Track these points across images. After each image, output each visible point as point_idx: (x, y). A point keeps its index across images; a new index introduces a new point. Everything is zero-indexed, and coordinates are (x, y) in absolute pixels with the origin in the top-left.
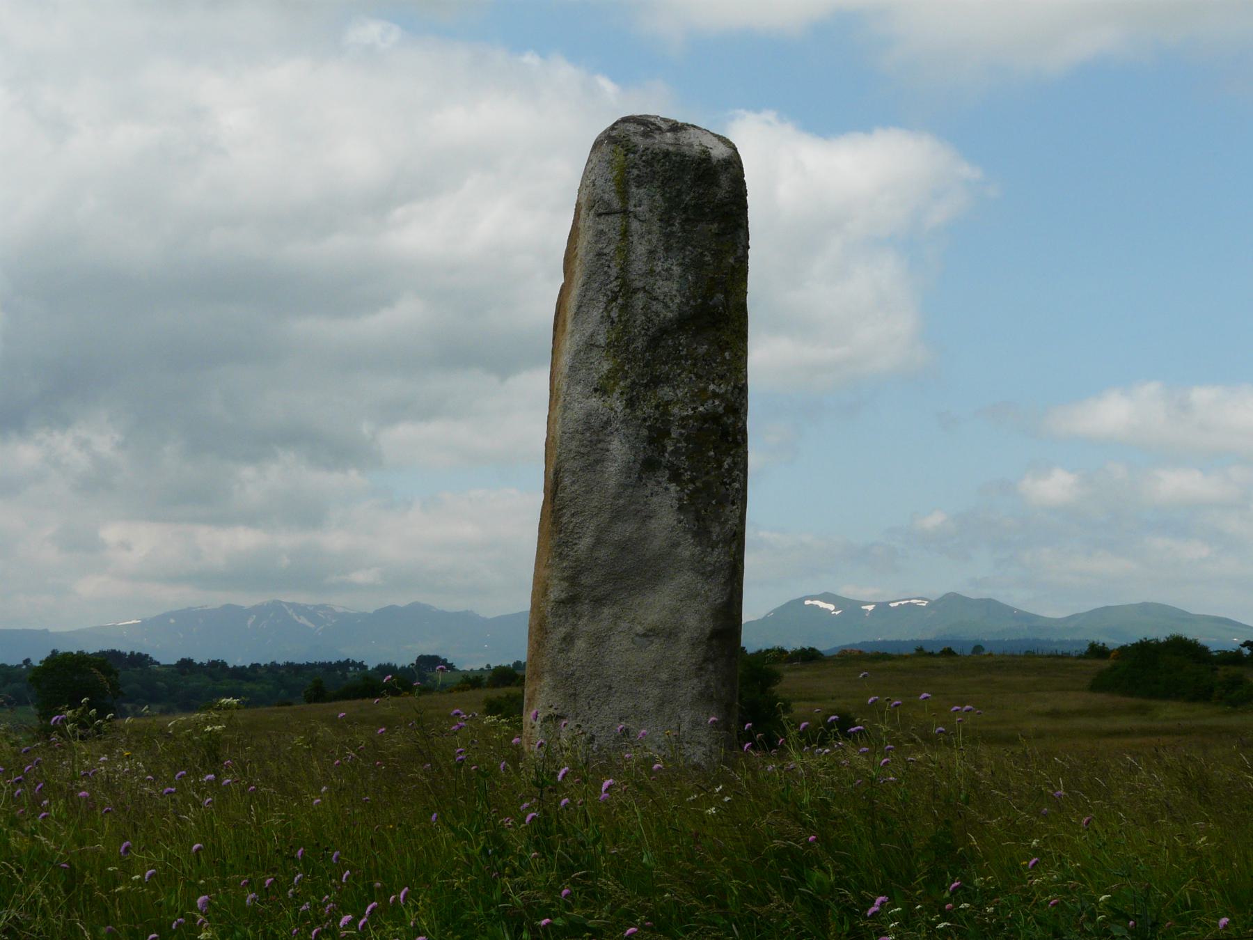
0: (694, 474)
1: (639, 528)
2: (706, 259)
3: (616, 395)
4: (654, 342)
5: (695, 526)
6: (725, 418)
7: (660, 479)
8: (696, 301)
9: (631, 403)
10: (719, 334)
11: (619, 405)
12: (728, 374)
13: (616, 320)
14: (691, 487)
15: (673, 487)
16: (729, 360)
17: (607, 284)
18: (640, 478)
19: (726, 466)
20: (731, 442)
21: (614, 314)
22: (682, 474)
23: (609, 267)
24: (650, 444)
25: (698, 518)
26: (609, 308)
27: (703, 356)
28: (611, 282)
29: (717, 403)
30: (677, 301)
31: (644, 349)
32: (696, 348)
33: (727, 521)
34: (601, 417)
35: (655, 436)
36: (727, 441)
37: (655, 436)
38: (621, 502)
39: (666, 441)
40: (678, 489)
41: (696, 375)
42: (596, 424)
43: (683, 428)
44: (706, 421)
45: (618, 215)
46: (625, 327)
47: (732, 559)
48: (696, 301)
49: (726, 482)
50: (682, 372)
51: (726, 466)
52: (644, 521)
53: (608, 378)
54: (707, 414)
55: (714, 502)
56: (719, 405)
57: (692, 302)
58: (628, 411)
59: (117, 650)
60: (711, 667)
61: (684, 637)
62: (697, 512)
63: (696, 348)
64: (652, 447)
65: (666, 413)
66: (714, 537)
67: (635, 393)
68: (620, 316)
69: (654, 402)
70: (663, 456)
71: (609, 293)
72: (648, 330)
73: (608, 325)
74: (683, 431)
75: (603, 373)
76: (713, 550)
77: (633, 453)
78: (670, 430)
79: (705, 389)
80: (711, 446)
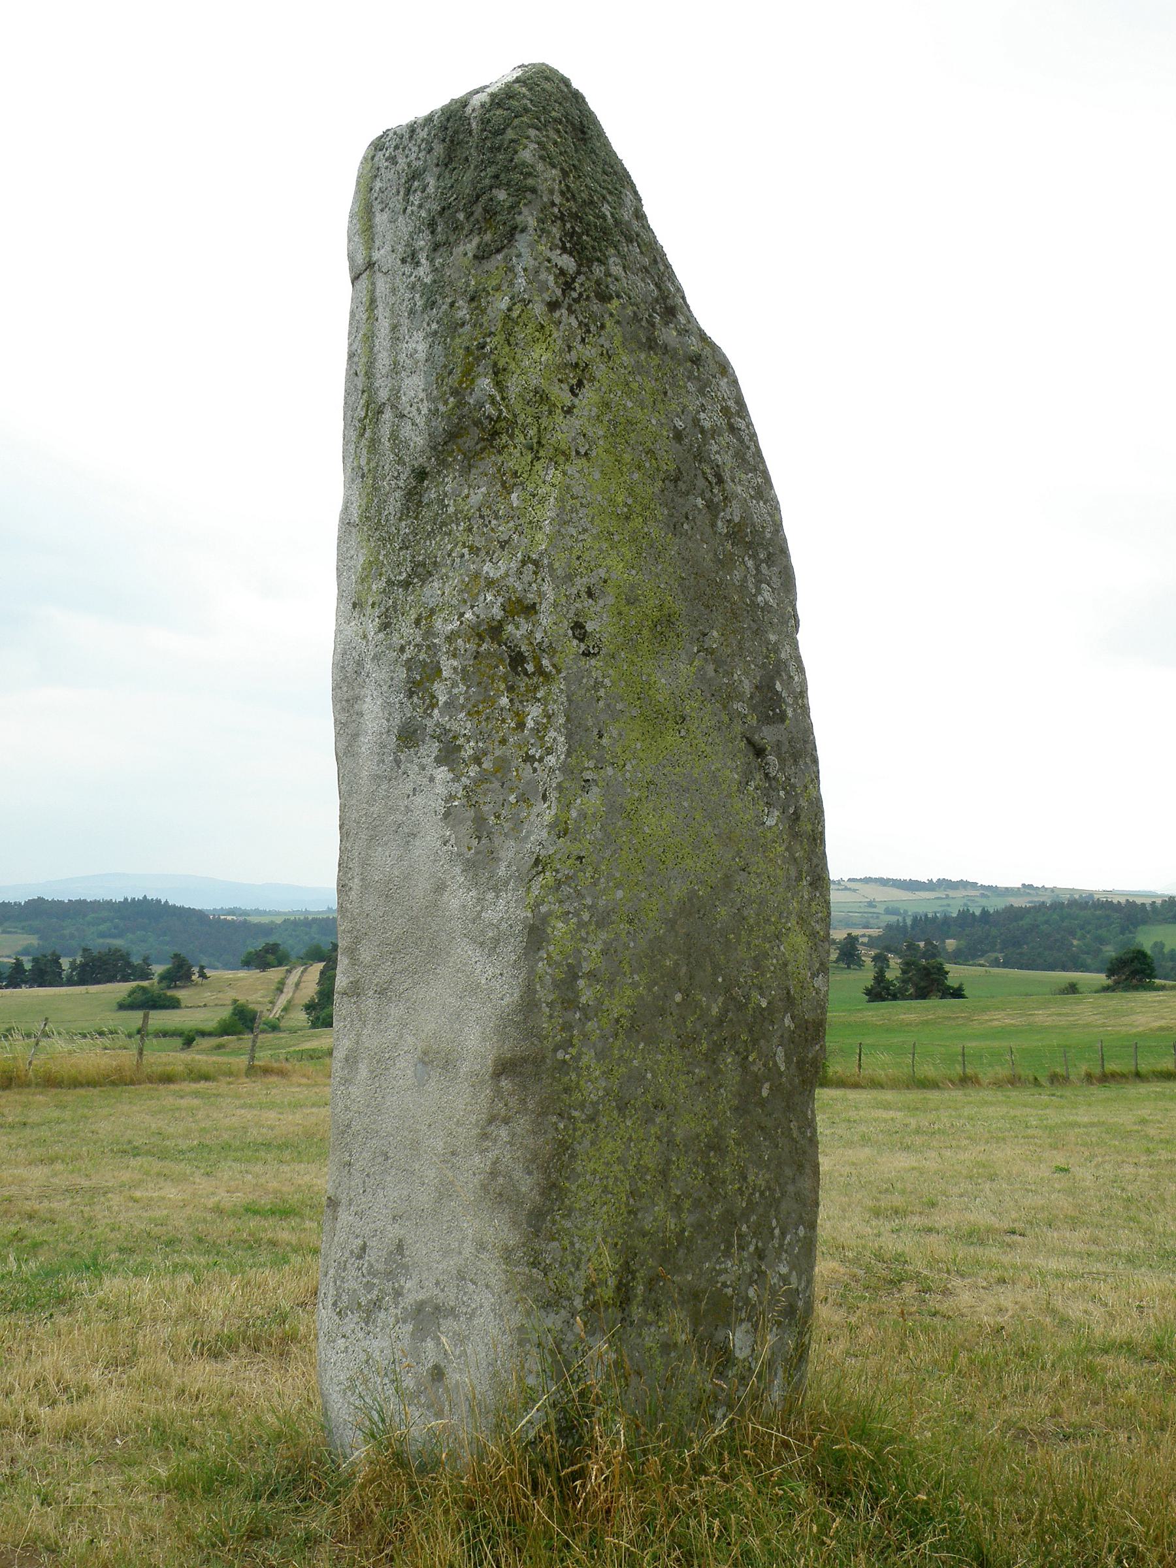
0: (480, 744)
1: (400, 858)
2: (461, 314)
3: (369, 610)
4: (413, 498)
7: (424, 761)
8: (446, 403)
10: (500, 459)
11: (372, 627)
12: (515, 537)
13: (366, 471)
14: (473, 771)
15: (442, 773)
16: (518, 508)
18: (398, 762)
20: (533, 674)
21: (363, 462)
22: (460, 748)
24: (410, 694)
25: (480, 827)
26: (358, 450)
27: (479, 510)
30: (425, 411)
32: (467, 496)
35: (418, 678)
36: (526, 673)
37: (418, 678)
39: (436, 685)
41: (471, 548)
43: (454, 656)
46: (374, 478)
47: (530, 915)
48: (446, 403)
49: (533, 756)
51: (530, 724)
52: (408, 842)
53: (363, 580)
54: (479, 624)
55: (512, 798)
56: (493, 603)
57: (442, 408)
58: (381, 635)
60: (504, 1133)
61: (464, 1068)
62: (480, 821)
63: (467, 496)
64: (415, 699)
65: (429, 633)
66: (502, 871)
67: (391, 601)
68: (368, 464)
74: (455, 664)
80: (503, 687)
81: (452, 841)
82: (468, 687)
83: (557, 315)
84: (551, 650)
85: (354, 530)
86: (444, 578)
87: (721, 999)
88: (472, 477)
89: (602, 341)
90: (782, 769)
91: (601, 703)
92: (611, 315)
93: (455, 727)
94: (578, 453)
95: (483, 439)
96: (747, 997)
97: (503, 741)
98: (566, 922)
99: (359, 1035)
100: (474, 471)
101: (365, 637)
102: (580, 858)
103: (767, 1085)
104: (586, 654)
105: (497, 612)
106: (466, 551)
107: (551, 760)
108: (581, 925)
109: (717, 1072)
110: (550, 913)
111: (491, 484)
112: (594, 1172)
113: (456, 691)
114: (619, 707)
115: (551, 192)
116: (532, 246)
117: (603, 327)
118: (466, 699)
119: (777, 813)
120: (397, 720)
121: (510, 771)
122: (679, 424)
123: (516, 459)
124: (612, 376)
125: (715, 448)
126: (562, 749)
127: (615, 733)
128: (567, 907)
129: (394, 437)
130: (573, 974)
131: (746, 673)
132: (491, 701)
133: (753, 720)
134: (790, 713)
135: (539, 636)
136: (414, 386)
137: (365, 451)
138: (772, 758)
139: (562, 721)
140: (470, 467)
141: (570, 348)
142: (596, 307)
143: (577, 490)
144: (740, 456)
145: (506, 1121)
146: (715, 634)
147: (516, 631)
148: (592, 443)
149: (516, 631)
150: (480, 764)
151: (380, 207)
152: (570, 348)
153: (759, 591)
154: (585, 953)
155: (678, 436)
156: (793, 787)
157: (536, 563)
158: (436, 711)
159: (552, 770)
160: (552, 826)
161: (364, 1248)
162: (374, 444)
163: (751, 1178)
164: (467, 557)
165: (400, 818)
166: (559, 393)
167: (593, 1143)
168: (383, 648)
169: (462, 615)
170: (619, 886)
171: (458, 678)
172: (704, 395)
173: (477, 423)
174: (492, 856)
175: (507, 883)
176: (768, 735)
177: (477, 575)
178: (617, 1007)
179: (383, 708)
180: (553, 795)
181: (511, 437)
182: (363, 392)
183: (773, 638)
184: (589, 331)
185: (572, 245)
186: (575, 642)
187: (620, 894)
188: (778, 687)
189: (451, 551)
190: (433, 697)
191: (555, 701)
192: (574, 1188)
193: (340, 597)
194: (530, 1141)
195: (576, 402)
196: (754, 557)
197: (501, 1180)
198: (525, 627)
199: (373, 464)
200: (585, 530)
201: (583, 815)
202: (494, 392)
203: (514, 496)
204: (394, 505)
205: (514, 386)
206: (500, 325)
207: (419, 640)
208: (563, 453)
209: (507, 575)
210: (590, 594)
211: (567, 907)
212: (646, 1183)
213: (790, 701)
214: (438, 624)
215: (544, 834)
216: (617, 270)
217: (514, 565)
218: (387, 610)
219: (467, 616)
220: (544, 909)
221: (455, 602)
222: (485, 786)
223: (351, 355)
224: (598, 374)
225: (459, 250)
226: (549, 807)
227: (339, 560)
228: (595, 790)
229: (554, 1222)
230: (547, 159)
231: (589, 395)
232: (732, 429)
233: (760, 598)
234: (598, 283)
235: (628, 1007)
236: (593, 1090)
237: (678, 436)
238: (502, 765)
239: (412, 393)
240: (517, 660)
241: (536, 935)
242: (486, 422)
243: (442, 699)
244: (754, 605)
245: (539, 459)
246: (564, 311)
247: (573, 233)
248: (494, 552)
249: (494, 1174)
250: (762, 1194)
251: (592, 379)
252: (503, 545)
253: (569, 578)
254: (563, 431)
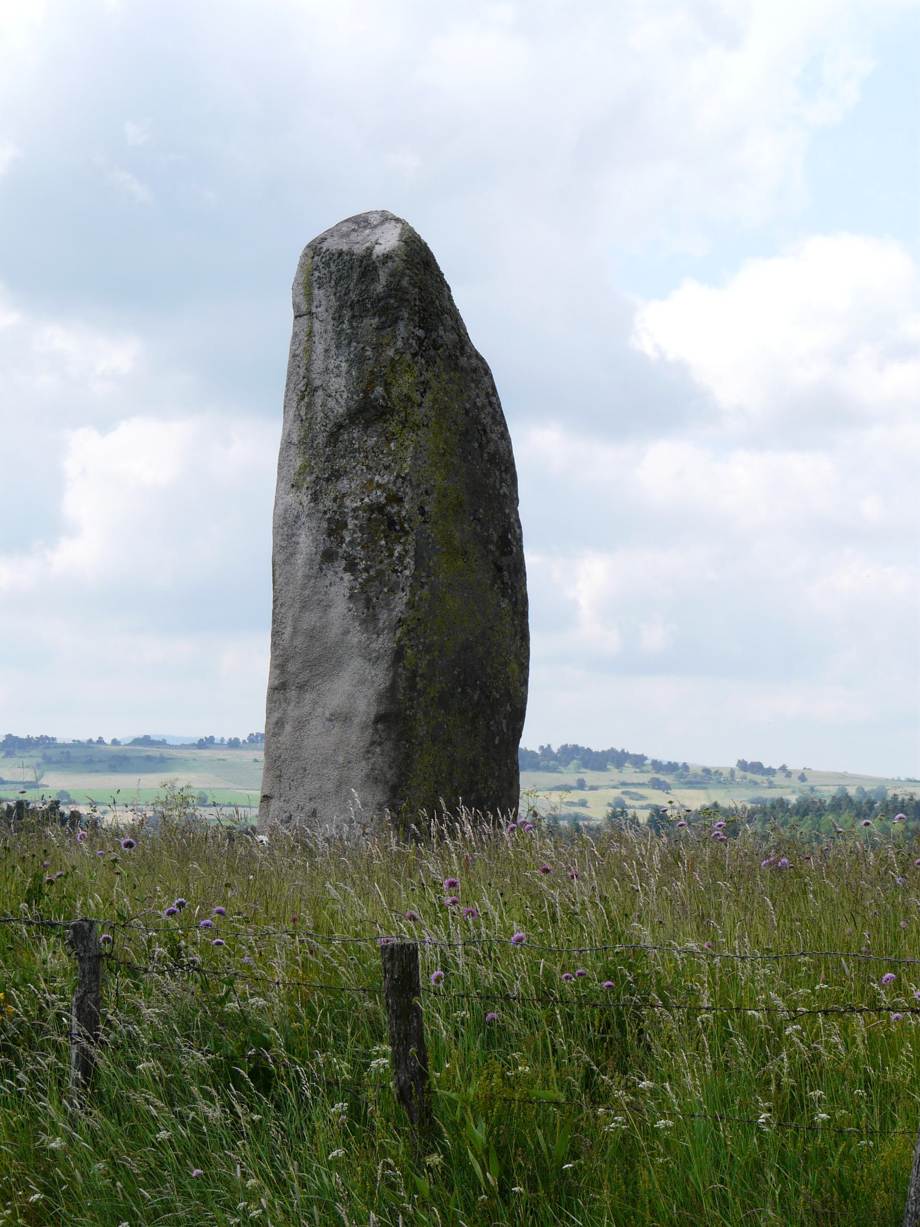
0: (369, 563)
1: (321, 618)
2: (368, 353)
3: (304, 490)
4: (333, 438)
5: (363, 613)
6: (389, 508)
7: (337, 570)
8: (358, 396)
9: (315, 498)
10: (385, 425)
11: (306, 500)
12: (393, 464)
13: (304, 418)
14: (365, 575)
15: (347, 576)
16: (394, 451)
18: (321, 569)
19: (396, 554)
20: (399, 531)
21: (303, 413)
22: (357, 564)
24: (329, 535)
25: (368, 603)
26: (299, 407)
27: (373, 448)
29: (379, 493)
30: (345, 396)
31: (325, 445)
32: (366, 441)
33: (393, 610)
36: (395, 530)
38: (307, 592)
39: (344, 532)
40: (352, 578)
41: (367, 466)
42: (291, 519)
43: (356, 519)
44: (372, 512)
45: (305, 317)
46: (310, 424)
47: (395, 645)
49: (397, 570)
50: (358, 464)
51: (396, 554)
52: (326, 610)
53: (300, 474)
54: (373, 505)
55: (386, 590)
56: (381, 496)
57: (355, 397)
58: (312, 504)
59: (619, 750)
60: (378, 750)
61: (356, 720)
62: (368, 601)
63: (366, 441)
64: (332, 538)
66: (381, 625)
67: (318, 487)
68: (306, 414)
69: (332, 495)
70: (341, 547)
72: (325, 426)
74: (357, 522)
76: (378, 637)
77: (315, 545)
78: (346, 521)
79: (371, 481)
80: (382, 536)
81: (354, 610)
82: (363, 534)
83: (416, 359)
84: (410, 520)
85: (293, 446)
86: (351, 480)
87: (478, 692)
88: (369, 432)
89: (435, 369)
90: (510, 579)
91: (430, 546)
92: (439, 356)
93: (355, 553)
94: (423, 425)
95: (376, 415)
96: (491, 692)
97: (381, 562)
98: (412, 650)
99: (285, 710)
100: (370, 429)
101: (301, 504)
102: (419, 620)
103: (498, 738)
104: (425, 522)
105: (382, 500)
106: (364, 468)
107: (407, 572)
108: (419, 652)
109: (476, 728)
110: (405, 645)
111: (379, 436)
112: (420, 770)
113: (355, 536)
114: (438, 547)
115: (415, 300)
116: (406, 326)
117: (436, 362)
118: (361, 540)
119: (507, 601)
120: (322, 548)
121: (384, 576)
122: (468, 406)
123: (393, 427)
124: (439, 385)
125: (483, 416)
126: (412, 566)
127: (436, 559)
128: (412, 643)
129: (324, 405)
130: (414, 674)
131: (494, 530)
132: (375, 542)
133: (497, 554)
134: (514, 550)
135: (404, 513)
136: (338, 383)
137: (304, 408)
138: (506, 573)
139: (412, 554)
140: (368, 427)
141: (421, 374)
142: (432, 352)
143: (422, 443)
144: (493, 418)
145: (380, 744)
146: (481, 510)
147: (393, 509)
148: (430, 420)
149: (393, 509)
150: (368, 573)
151: (318, 286)
152: (421, 374)
153: (501, 487)
154: (420, 665)
155: (467, 412)
156: (515, 588)
157: (403, 478)
158: (344, 545)
159: (407, 577)
160: (407, 604)
161: (290, 817)
162: (310, 406)
163: (489, 783)
164: (365, 471)
165: (321, 597)
166: (417, 397)
167: (420, 756)
168: (313, 511)
169: (363, 499)
170: (435, 634)
171: (358, 529)
172: (478, 388)
173: (374, 407)
174: (375, 618)
175: (383, 631)
176: (504, 561)
177: (371, 481)
178: (433, 692)
179: (313, 542)
180: (408, 589)
181: (392, 416)
182: (304, 378)
183: (507, 511)
184: (429, 365)
185: (423, 324)
186: (420, 517)
187: (435, 638)
188: (510, 537)
189: (355, 466)
190: (342, 537)
191: (410, 544)
192: (411, 776)
193: (280, 478)
194: (392, 754)
195: (423, 400)
196: (499, 470)
197: (377, 772)
198: (396, 508)
199: (309, 416)
200: (425, 462)
201: (421, 599)
202: (384, 394)
203: (392, 445)
204: (321, 439)
205: (395, 391)
206: (389, 362)
207: (335, 508)
208: (417, 426)
209: (388, 483)
210: (427, 493)
211: (412, 643)
212: (442, 777)
213: (515, 543)
214: (348, 502)
215: (403, 607)
216: (441, 333)
217: (392, 478)
218: (316, 491)
219: (366, 500)
220: (402, 643)
221: (358, 492)
222: (371, 583)
223: (294, 356)
224: (433, 385)
225: (367, 321)
226: (406, 595)
227: (279, 461)
228: (426, 587)
229: (402, 791)
230: (414, 285)
231: (429, 395)
232: (491, 403)
233: (502, 491)
234: (434, 340)
235: (437, 692)
236: (421, 730)
237: (467, 412)
238: (380, 573)
239: (337, 386)
240: (391, 524)
241: (398, 655)
242: (379, 408)
243: (348, 539)
244: (499, 494)
245: (405, 427)
246: (419, 357)
247: (424, 318)
248: (381, 470)
249: (373, 770)
250: (494, 792)
251: (430, 388)
252: (387, 468)
253: (418, 485)
254: (418, 415)
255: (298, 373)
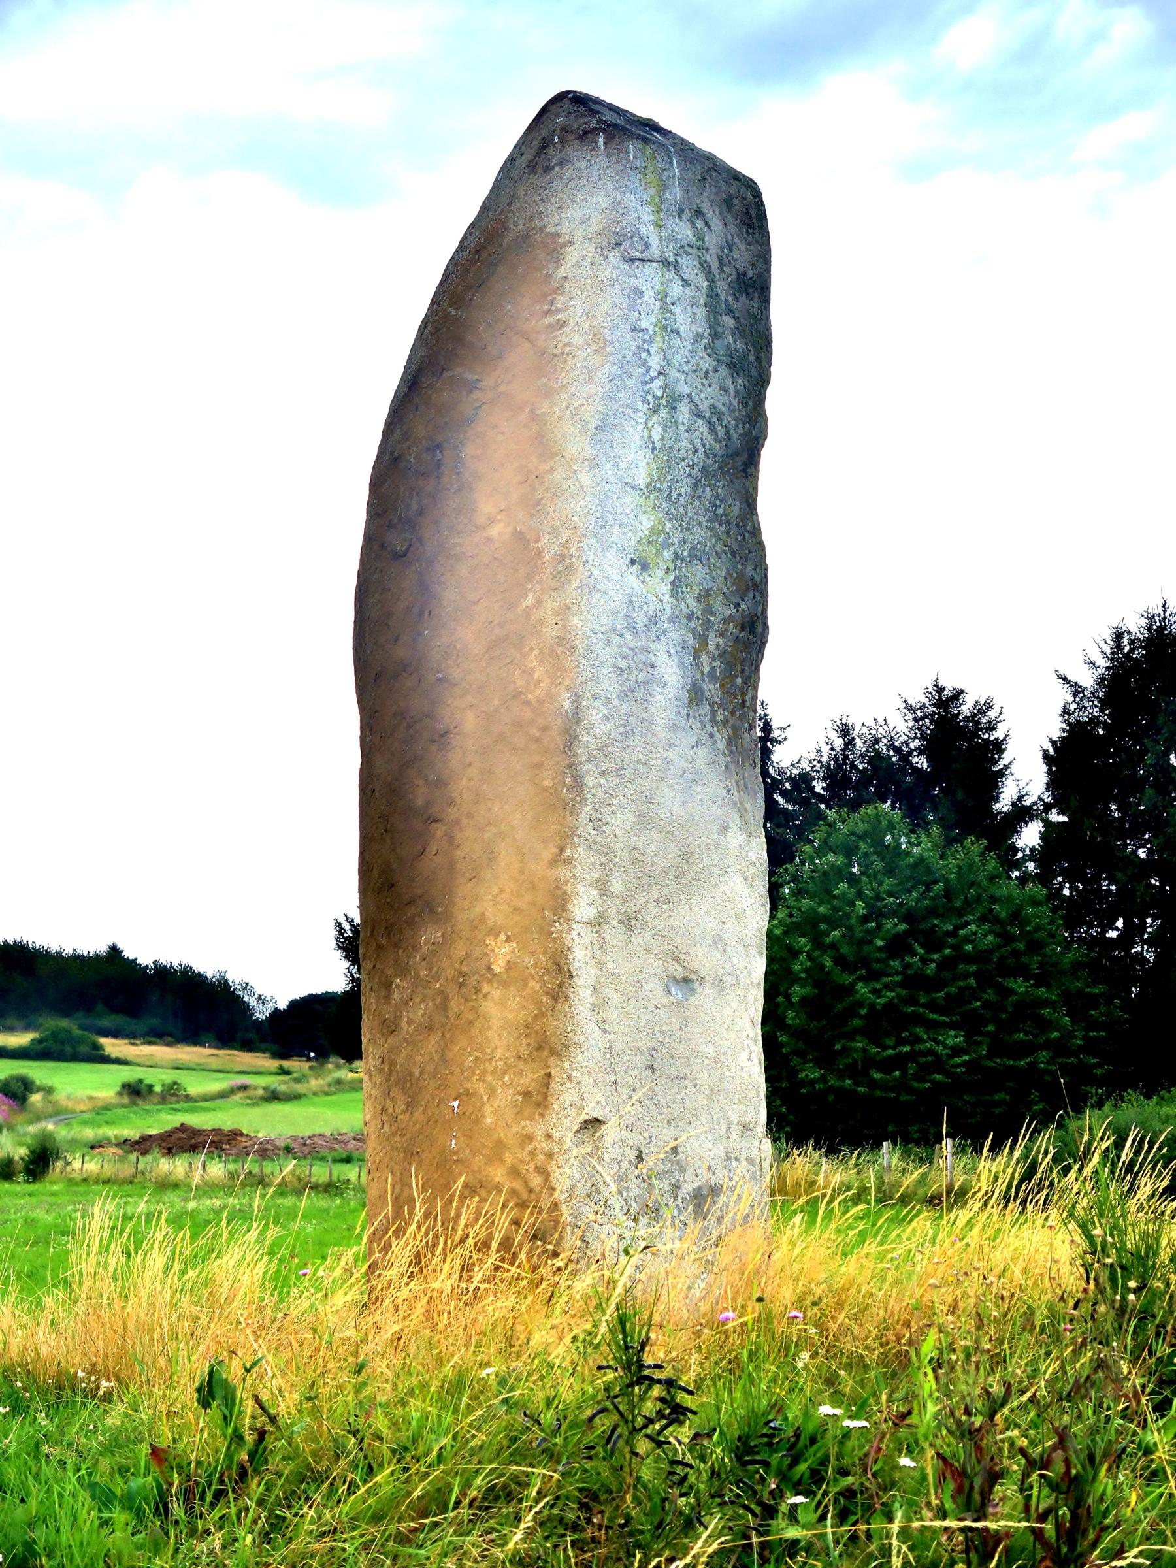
13: (658, 445)
17: (646, 383)
18: (688, 716)
21: (657, 433)
23: (648, 351)
28: (652, 380)
34: (645, 607)
71: (650, 397)
73: (649, 454)
75: (640, 534)
255: (644, 363)
